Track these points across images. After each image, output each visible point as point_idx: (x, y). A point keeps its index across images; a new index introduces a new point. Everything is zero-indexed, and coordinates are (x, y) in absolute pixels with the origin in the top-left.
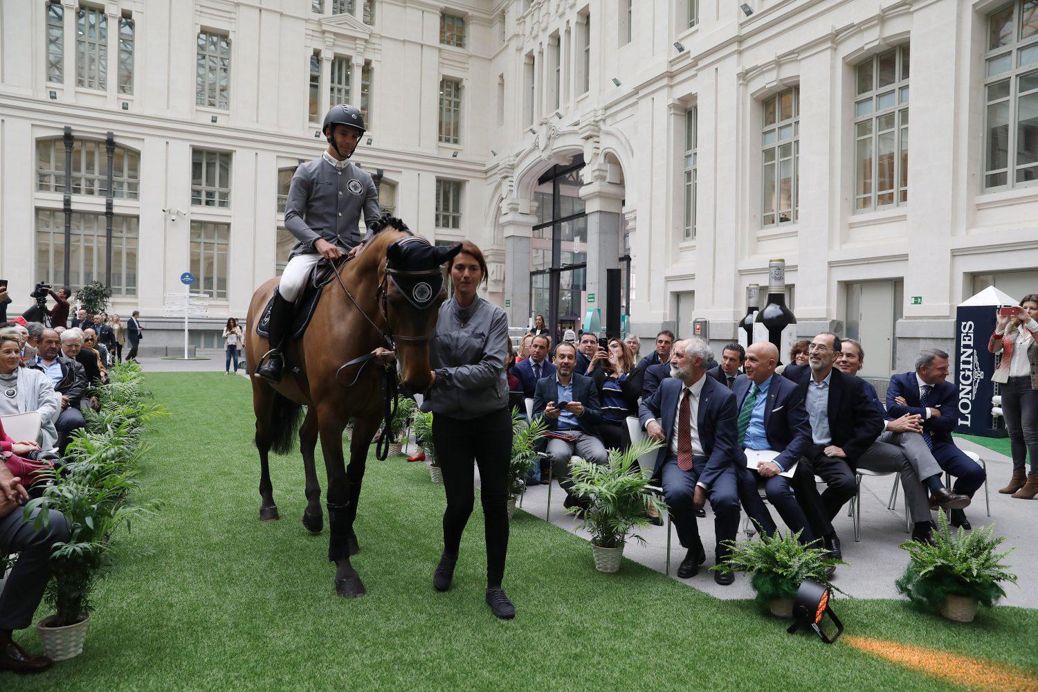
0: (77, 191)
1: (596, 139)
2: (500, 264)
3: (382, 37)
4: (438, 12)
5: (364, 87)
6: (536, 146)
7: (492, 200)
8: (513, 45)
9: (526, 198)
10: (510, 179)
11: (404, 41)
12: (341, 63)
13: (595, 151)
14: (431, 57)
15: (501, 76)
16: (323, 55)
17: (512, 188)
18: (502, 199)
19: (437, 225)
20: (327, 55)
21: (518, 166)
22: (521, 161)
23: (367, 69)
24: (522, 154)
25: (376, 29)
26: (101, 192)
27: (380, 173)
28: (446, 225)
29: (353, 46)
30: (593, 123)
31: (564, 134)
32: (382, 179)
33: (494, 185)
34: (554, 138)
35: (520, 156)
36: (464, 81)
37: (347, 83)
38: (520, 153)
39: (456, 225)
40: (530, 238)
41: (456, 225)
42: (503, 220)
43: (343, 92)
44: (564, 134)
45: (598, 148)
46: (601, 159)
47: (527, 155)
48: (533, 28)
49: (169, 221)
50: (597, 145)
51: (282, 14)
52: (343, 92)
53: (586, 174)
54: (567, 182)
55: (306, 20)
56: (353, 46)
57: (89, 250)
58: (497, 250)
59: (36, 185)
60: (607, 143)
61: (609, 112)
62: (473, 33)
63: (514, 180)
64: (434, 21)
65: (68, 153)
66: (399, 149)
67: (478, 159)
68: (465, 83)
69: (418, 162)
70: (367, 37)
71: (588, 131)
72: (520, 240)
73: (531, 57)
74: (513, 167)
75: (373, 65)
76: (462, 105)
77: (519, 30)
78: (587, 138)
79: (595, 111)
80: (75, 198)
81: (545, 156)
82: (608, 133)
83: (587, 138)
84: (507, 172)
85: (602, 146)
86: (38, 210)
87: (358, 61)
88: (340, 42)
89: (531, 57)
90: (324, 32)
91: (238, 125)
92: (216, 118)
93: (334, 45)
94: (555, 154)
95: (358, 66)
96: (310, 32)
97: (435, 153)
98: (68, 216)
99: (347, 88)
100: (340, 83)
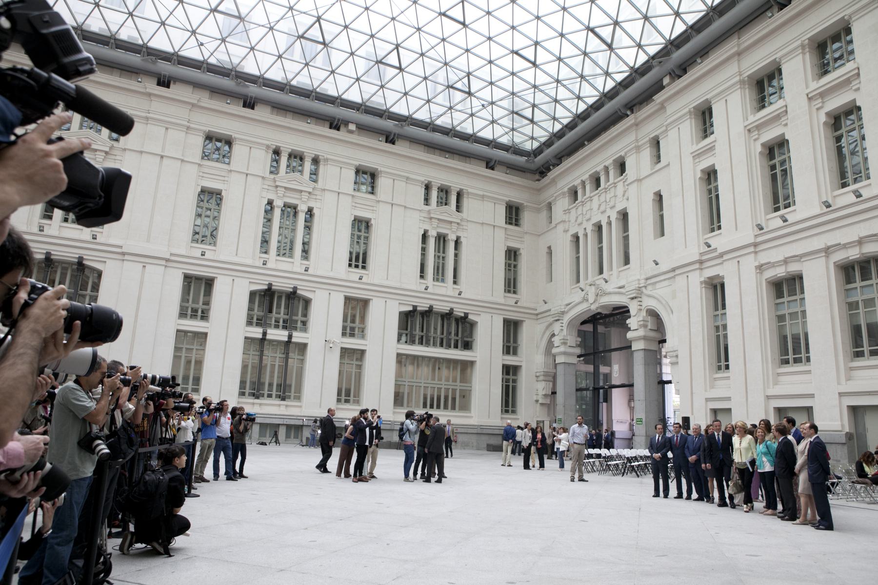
1: (639, 299)
3: (468, 221)
4: (505, 204)
5: (456, 255)
6: (585, 300)
8: (561, 228)
10: (561, 321)
11: (483, 224)
12: (441, 239)
13: (639, 307)
14: (500, 234)
15: (549, 248)
16: (430, 233)
17: (563, 328)
20: (433, 233)
21: (567, 312)
22: (570, 309)
23: (457, 243)
24: (572, 304)
25: (464, 214)
27: (466, 315)
29: (449, 227)
30: (637, 289)
31: (610, 293)
33: (546, 324)
34: (601, 295)
35: (570, 306)
36: (521, 250)
37: (444, 252)
38: (569, 304)
41: (515, 353)
42: (554, 351)
43: (441, 258)
44: (610, 293)
45: (641, 306)
46: (644, 313)
47: (573, 307)
48: (577, 217)
49: (328, 348)
50: (641, 303)
51: (405, 207)
52: (441, 258)
53: (632, 322)
54: (601, 324)
55: (420, 211)
56: (449, 227)
60: (649, 303)
61: (649, 282)
62: (526, 217)
63: (565, 323)
64: (502, 211)
66: (479, 298)
67: (532, 306)
68: (522, 251)
69: (490, 307)
70: (459, 221)
71: (634, 293)
73: (576, 238)
74: (563, 313)
75: (462, 239)
76: (519, 267)
77: (565, 217)
78: (632, 299)
79: (639, 280)
81: (593, 307)
82: (649, 296)
83: (632, 299)
84: (559, 317)
85: (644, 304)
87: (452, 237)
88: (442, 225)
89: (576, 238)
90: (431, 218)
91: (376, 282)
92: (362, 277)
93: (437, 226)
94: (601, 306)
95: (432, 236)
96: (423, 219)
97: (502, 301)
99: (444, 255)
100: (439, 252)
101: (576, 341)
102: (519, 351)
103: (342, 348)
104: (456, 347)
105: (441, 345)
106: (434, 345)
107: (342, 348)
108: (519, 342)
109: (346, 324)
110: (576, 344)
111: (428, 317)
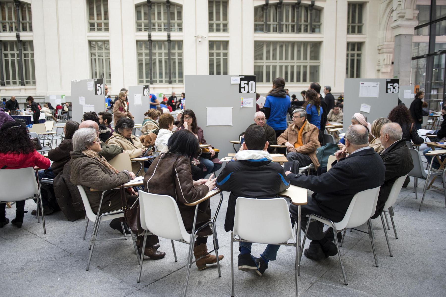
0: (154, 30)
2: (389, 54)
7: (384, 13)
9: (410, 9)
18: (393, 11)
19: (348, 32)
26: (165, 30)
28: (353, 32)
32: (314, 7)
39: (360, 32)
40: (412, 35)
41: (360, 32)
57: (160, 62)
58: (387, 45)
59: (136, 29)
65: (149, 11)
72: (406, 37)
80: (153, 34)
86: (137, 41)
98: (150, 43)
101: (414, 14)
102: (364, 29)
103: (210, 41)
104: (306, 31)
105: (293, 31)
106: (287, 31)
107: (210, 41)
108: (364, 21)
109: (211, 22)
110: (414, 17)
111: (280, 8)
